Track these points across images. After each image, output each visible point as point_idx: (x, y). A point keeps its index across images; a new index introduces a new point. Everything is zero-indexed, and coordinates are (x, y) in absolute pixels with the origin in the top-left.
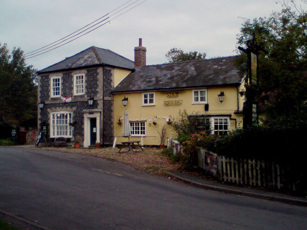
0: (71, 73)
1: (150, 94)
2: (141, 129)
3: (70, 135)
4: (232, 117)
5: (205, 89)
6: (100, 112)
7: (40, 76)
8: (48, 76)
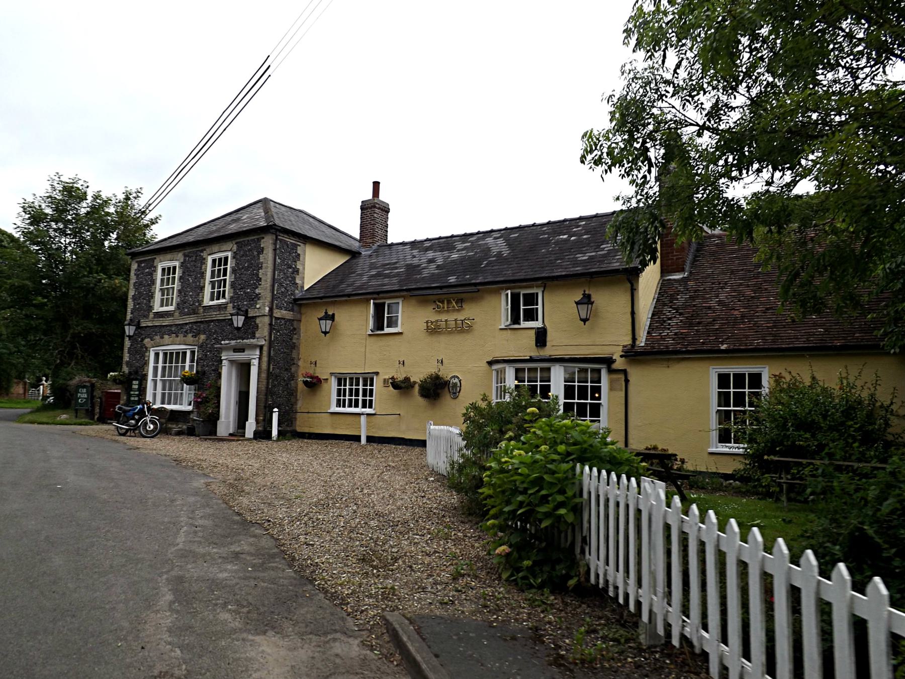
0: (202, 251)
2: (364, 395)
4: (615, 366)
5: (537, 287)
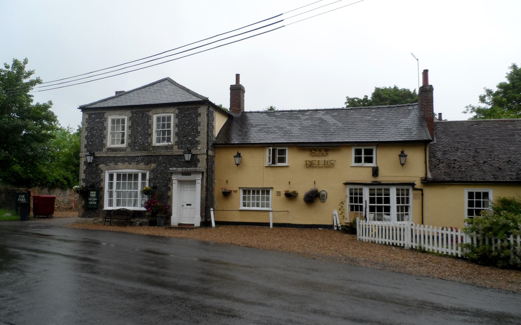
0: (148, 111)
1: (365, 150)
3: (398, 220)
4: (416, 187)
6: (203, 173)
7: (87, 114)
8: (103, 114)
